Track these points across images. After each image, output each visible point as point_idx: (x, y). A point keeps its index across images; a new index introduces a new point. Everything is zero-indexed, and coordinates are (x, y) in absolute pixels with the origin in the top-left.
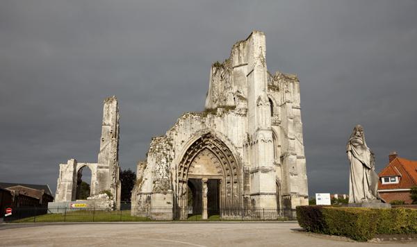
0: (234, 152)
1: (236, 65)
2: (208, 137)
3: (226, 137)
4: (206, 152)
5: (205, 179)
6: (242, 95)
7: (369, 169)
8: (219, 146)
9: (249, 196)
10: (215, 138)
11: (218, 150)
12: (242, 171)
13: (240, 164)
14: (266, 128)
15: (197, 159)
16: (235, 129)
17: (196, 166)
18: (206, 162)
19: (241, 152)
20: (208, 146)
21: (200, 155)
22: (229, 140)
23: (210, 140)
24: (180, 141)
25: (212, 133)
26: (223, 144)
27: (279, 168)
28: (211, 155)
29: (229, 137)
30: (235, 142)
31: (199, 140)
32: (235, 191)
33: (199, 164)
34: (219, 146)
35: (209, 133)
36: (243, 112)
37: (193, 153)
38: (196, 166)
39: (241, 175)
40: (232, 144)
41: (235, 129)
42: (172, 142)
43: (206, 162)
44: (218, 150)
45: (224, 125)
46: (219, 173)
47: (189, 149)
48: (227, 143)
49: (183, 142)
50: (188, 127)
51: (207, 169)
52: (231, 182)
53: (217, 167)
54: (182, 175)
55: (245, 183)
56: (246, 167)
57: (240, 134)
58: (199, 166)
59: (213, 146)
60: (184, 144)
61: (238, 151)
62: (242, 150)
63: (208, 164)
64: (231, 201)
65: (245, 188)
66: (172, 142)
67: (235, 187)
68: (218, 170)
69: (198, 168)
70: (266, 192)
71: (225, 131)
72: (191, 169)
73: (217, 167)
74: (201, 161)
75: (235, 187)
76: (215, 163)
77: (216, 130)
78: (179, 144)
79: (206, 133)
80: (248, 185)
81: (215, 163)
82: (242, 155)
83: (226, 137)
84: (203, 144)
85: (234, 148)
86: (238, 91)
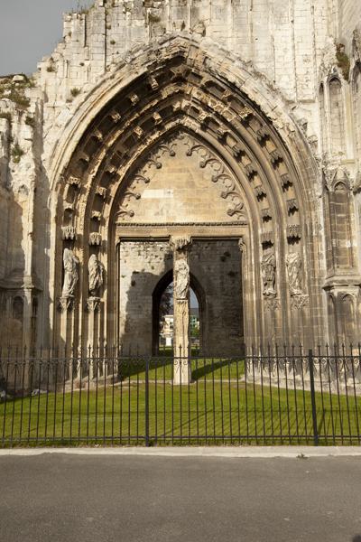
0: (282, 120)
2: (180, 80)
3: (250, 63)
4: (183, 144)
5: (181, 237)
8: (224, 110)
10: (207, 78)
11: (223, 129)
12: (318, 189)
13: (309, 163)
15: (149, 171)
16: (283, 35)
17: (147, 193)
18: (184, 176)
19: (315, 121)
20: (187, 121)
21: (162, 156)
22: (257, 75)
23: (187, 88)
24: (65, 91)
25: (192, 56)
26: (236, 95)
28: (202, 154)
29: (260, 67)
30: (285, 83)
31: (140, 85)
32: (291, 274)
33: (157, 186)
34: (224, 110)
35: (179, 59)
37: (132, 142)
38: (147, 193)
39: (311, 207)
40: (272, 88)
41: (283, 35)
42: (28, 93)
43: (184, 176)
44: (223, 129)
45: (239, 23)
46: (232, 213)
47: (102, 121)
48: (251, 88)
49: (75, 93)
50: (96, 40)
51: (189, 202)
52: (277, 240)
53: (224, 196)
54: (80, 221)
55: (333, 234)
56: (337, 169)
57: (305, 49)
58: (159, 194)
59: (204, 115)
60: (80, 98)
61: (299, 114)
62: (315, 108)
63: (191, 184)
64: (278, 312)
65: (335, 256)
66: (28, 93)
67: (292, 255)
68: (231, 206)
69: (156, 201)
71: (242, 42)
72: (128, 204)
73: (224, 196)
74: (163, 175)
76: (215, 180)
77: (202, 43)
78: (61, 103)
79: (165, 55)
80: (347, 244)
81: (215, 180)
82: (314, 130)
83: (250, 63)
84: (169, 114)
85: (280, 105)
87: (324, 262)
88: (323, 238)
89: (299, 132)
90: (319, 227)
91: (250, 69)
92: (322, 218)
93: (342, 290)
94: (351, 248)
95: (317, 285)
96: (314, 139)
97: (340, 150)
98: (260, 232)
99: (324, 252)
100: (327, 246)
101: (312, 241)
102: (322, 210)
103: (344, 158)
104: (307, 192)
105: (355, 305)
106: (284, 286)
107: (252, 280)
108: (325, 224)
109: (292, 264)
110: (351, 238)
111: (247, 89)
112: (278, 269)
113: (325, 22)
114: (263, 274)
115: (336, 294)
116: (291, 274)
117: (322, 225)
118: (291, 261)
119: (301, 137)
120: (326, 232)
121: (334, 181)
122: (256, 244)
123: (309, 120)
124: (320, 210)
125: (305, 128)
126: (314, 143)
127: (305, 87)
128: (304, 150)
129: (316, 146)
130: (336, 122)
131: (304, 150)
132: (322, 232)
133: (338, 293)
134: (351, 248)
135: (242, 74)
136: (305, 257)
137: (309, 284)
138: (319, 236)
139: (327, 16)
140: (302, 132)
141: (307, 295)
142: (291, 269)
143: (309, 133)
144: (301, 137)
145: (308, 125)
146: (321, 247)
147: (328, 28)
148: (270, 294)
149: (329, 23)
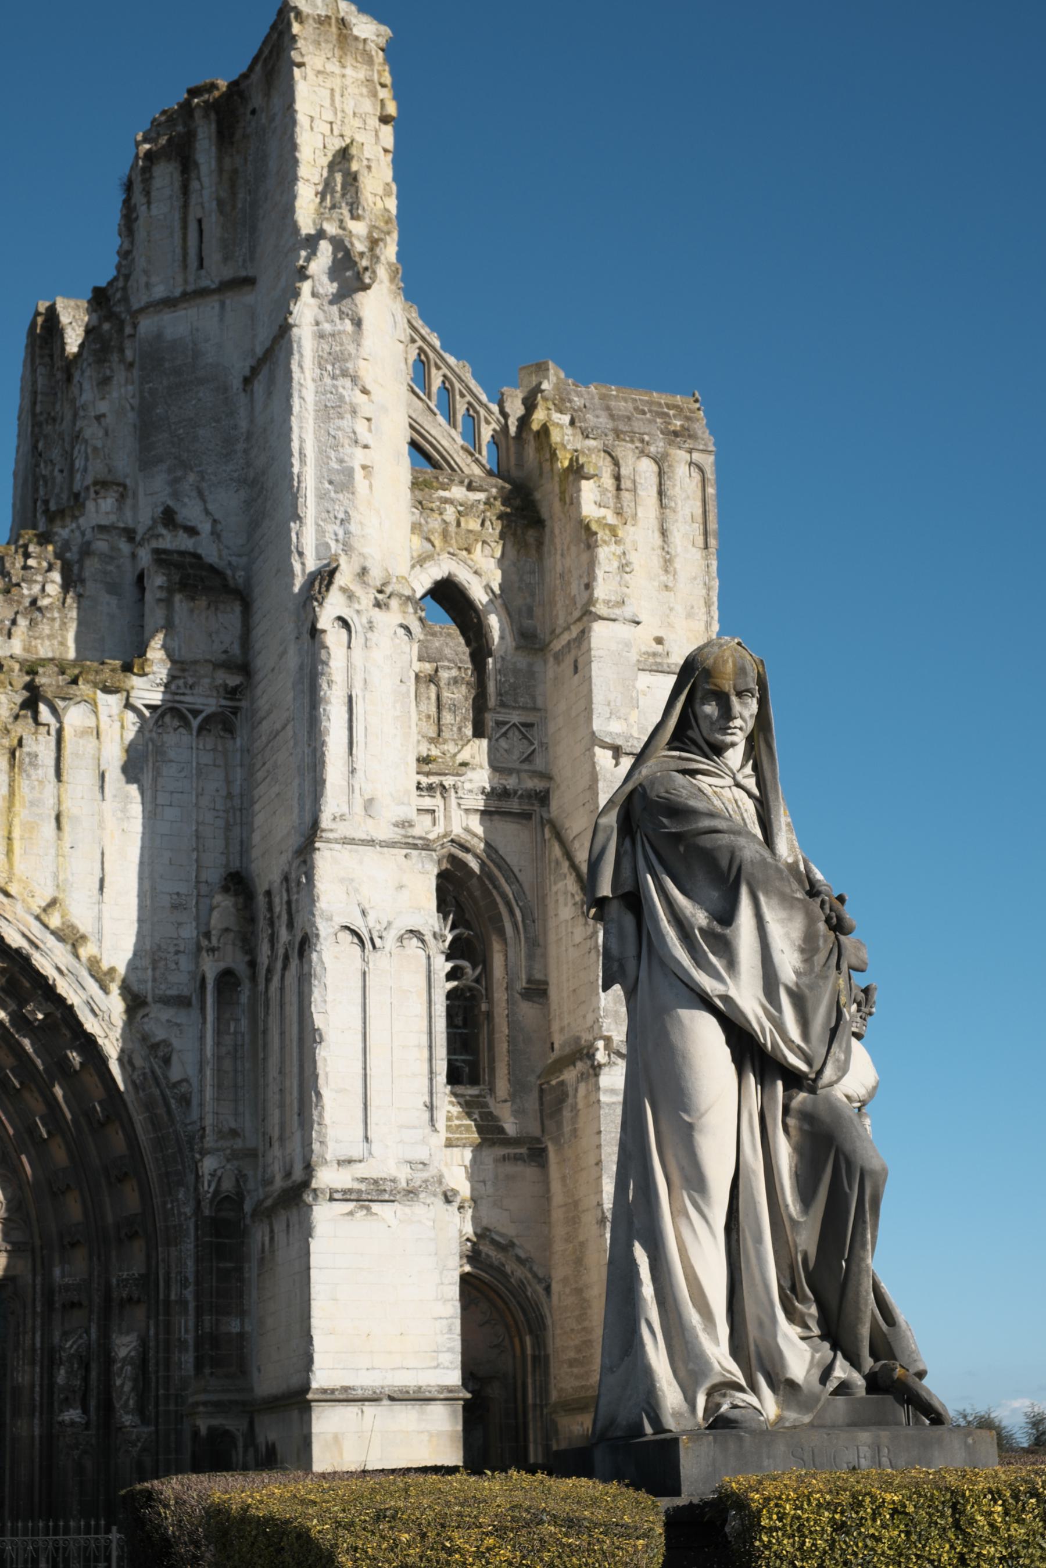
1: (159, 292)
6: (210, 552)
7: (794, 1080)
9: (235, 1425)
14: (385, 832)
27: (530, 1172)
32: (124, 1383)
36: (210, 704)
70: (364, 1380)
75: (125, 1346)
86: (169, 518)
87: (188, 1359)
88: (192, 1306)
89: (153, 1072)
90: (184, 1284)
91: (55, 921)
92: (190, 1263)
93: (215, 1422)
94: (241, 1335)
95: (172, 1407)
96: (184, 1088)
97: (233, 1125)
98: (57, 1272)
99: (190, 1338)
100: (197, 1326)
101: (168, 1313)
102: (191, 1246)
103: (238, 1144)
104: (165, 1203)
105: (241, 1450)
106: (107, 1407)
107: (33, 1386)
108: (197, 1277)
109: (124, 1359)
110: (242, 1314)
111: (42, 964)
112: (94, 1366)
113: (220, 823)
114: (61, 1376)
115: (203, 1431)
116: (124, 1383)
117: (191, 1279)
118: (122, 1353)
119: (158, 1084)
120: (198, 1296)
121: (217, 1192)
122: (49, 1304)
123: (176, 1043)
124: (189, 1246)
125: (167, 1061)
126: (185, 1101)
127: (174, 966)
128: (161, 1111)
129: (188, 1103)
130: (228, 1064)
131: (161, 1111)
132: (189, 1294)
133: (211, 1429)
134: (241, 1335)
135: (36, 929)
136: (152, 1344)
137: (157, 1405)
138: (183, 1302)
139: (226, 811)
140: (158, 1071)
141: (153, 1428)
142: (121, 1369)
143: (175, 1073)
144: (158, 1084)
145: (175, 1059)
146: (185, 1327)
147: (227, 839)
148: (73, 1423)
149: (228, 828)
